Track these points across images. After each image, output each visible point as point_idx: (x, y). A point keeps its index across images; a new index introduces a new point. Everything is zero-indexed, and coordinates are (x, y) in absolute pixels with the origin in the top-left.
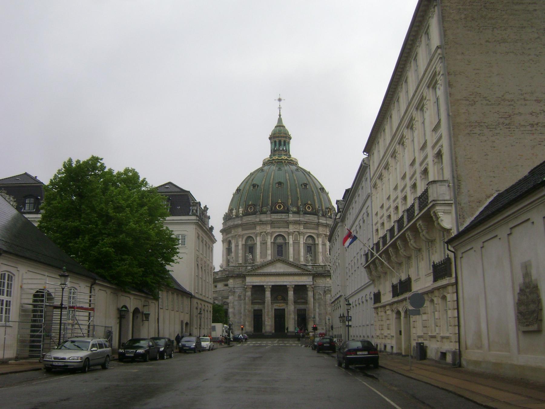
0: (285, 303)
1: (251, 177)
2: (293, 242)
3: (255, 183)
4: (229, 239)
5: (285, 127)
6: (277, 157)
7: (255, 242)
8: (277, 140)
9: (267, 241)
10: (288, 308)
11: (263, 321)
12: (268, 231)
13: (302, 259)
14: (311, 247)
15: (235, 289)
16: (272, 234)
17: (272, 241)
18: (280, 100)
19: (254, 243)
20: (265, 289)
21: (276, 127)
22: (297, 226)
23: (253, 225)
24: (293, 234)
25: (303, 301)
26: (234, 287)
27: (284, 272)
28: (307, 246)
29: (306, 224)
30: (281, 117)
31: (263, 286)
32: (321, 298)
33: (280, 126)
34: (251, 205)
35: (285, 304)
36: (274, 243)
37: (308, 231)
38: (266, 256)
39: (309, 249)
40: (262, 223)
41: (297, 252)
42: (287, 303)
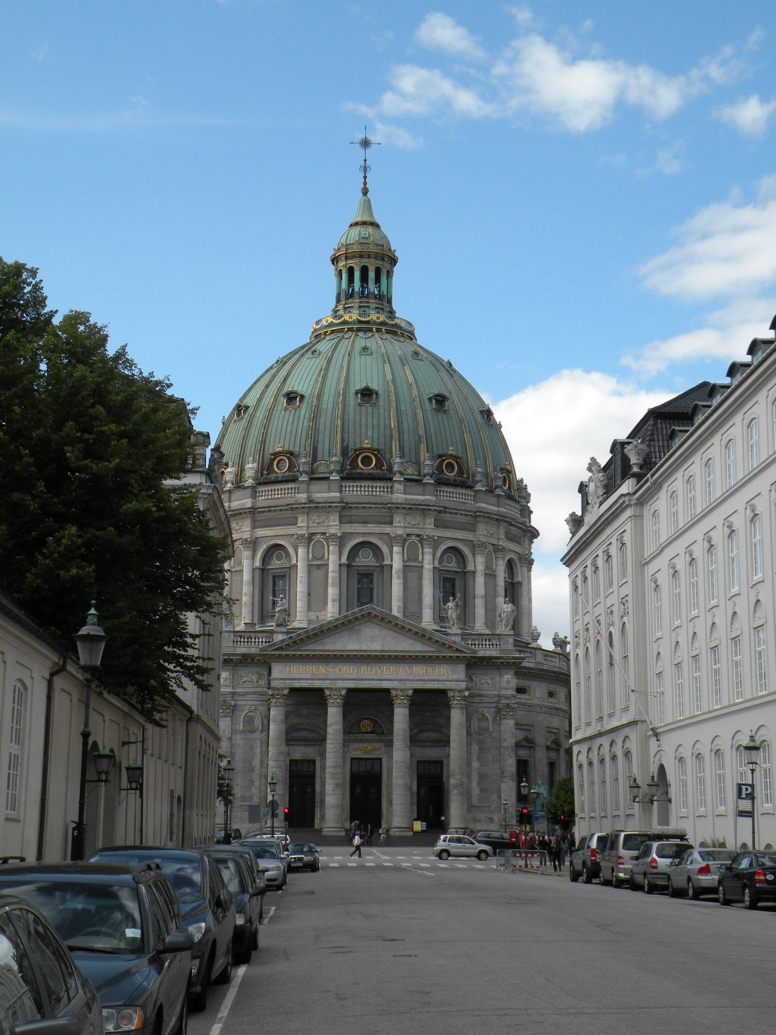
0: (381, 741)
1: (278, 371)
2: (404, 566)
5: (378, 226)
6: (354, 318)
7: (294, 562)
10: (391, 757)
12: (333, 531)
14: (454, 580)
15: (236, 697)
16: (341, 540)
17: (344, 560)
20: (327, 700)
21: (351, 226)
22: (416, 519)
24: (405, 540)
25: (434, 735)
26: (234, 694)
27: (382, 651)
28: (445, 579)
31: (321, 691)
32: (488, 728)
33: (364, 223)
35: (382, 745)
36: (348, 567)
37: (448, 533)
38: (326, 604)
39: (448, 585)
40: (313, 507)
41: (412, 594)
42: (392, 741)
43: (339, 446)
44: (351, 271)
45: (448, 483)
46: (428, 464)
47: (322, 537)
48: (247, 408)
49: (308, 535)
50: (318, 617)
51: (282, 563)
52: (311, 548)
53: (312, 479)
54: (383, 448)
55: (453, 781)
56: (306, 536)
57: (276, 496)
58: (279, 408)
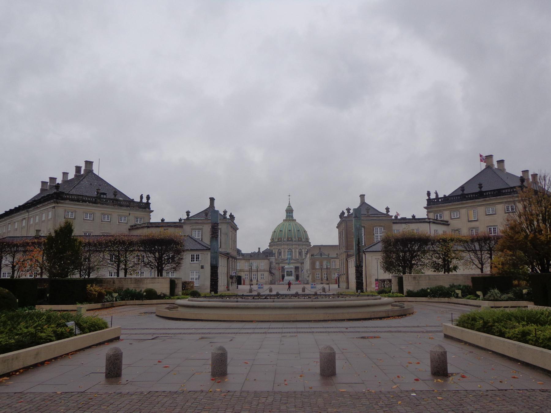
8: (288, 212)
13: (297, 257)
16: (287, 248)
18: (289, 196)
23: (281, 245)
29: (299, 245)
37: (300, 247)
40: (284, 245)
41: (296, 254)
45: (299, 241)
46: (297, 239)
55: (300, 275)
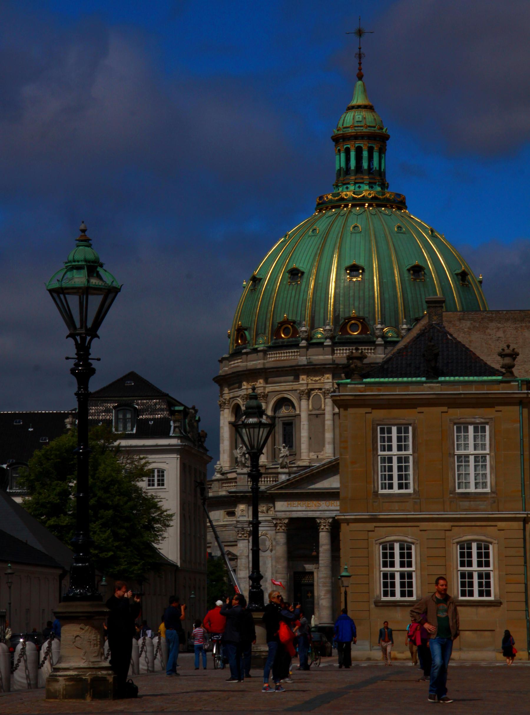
3: (294, 265)
4: (235, 402)
6: (350, 194)
9: (324, 410)
11: (316, 598)
12: (328, 386)
18: (360, 33)
19: (293, 414)
30: (363, 79)
31: (313, 519)
33: (359, 107)
34: (286, 322)
38: (324, 446)
43: (330, 316)
44: (347, 151)
47: (319, 391)
48: (260, 280)
49: (308, 390)
50: (318, 457)
51: (289, 412)
52: (310, 400)
53: (311, 345)
54: (367, 316)
56: (307, 391)
57: (283, 358)
58: (285, 283)
